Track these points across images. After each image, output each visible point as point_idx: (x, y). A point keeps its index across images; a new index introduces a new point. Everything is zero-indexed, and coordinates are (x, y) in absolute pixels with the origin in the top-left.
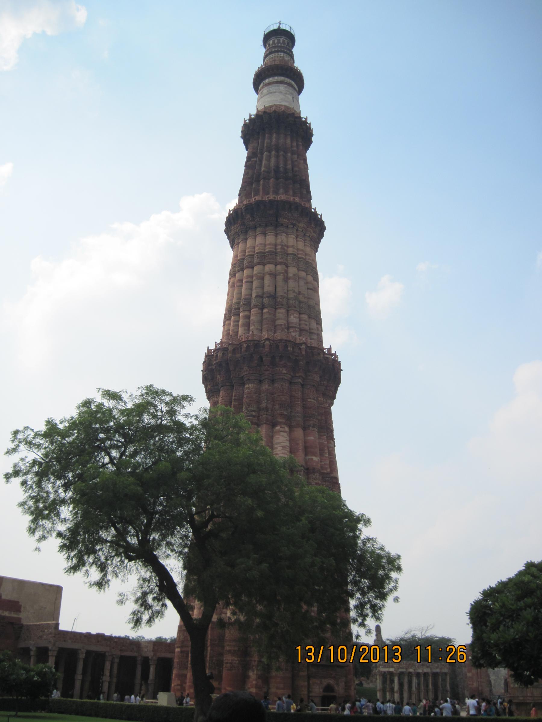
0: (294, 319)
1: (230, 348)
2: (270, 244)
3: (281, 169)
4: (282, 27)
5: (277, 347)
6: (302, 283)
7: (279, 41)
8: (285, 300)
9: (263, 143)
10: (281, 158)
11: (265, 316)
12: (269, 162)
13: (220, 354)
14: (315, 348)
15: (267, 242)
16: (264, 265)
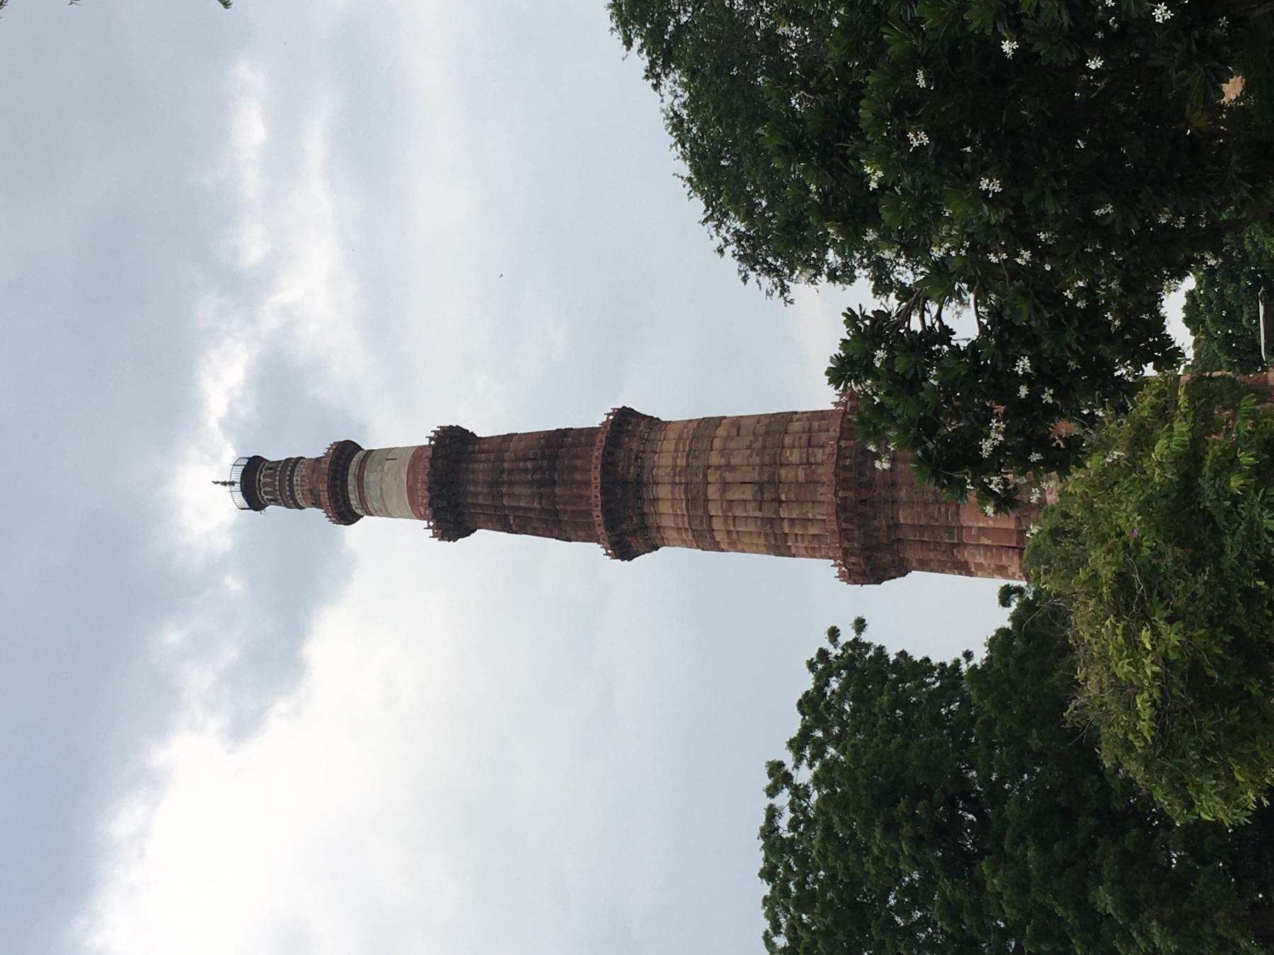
0: (794, 456)
1: (846, 544)
2: (673, 493)
3: (537, 476)
4: (237, 477)
5: (844, 479)
6: (732, 445)
7: (265, 485)
8: (766, 468)
9: (482, 506)
10: (515, 477)
11: (793, 497)
12: (523, 497)
13: (853, 560)
14: (841, 427)
15: (670, 496)
16: (707, 500)
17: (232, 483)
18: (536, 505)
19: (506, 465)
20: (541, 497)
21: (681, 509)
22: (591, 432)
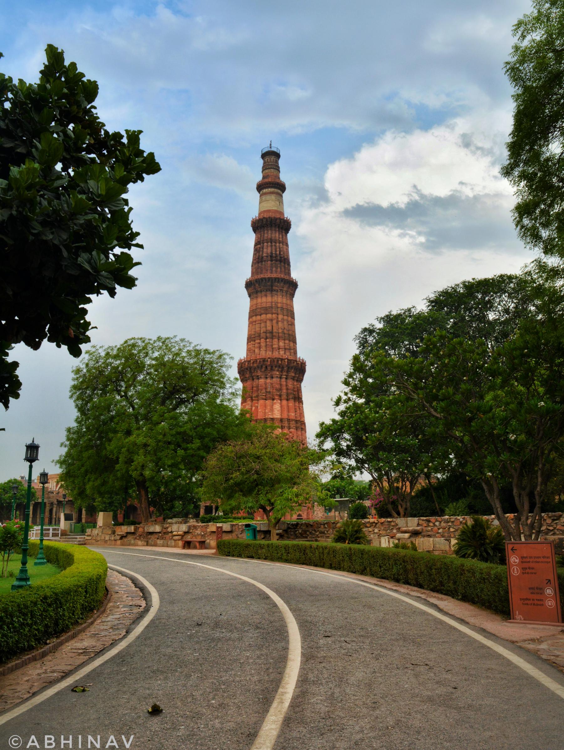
0: (281, 344)
1: (252, 362)
3: (274, 255)
4: (273, 149)
6: (285, 323)
7: (270, 159)
9: (264, 236)
10: (273, 247)
11: (268, 343)
12: (267, 250)
13: (247, 364)
16: (266, 314)
17: (271, 148)
18: (264, 255)
19: (278, 244)
20: (267, 257)
21: (264, 305)
22: (289, 274)
